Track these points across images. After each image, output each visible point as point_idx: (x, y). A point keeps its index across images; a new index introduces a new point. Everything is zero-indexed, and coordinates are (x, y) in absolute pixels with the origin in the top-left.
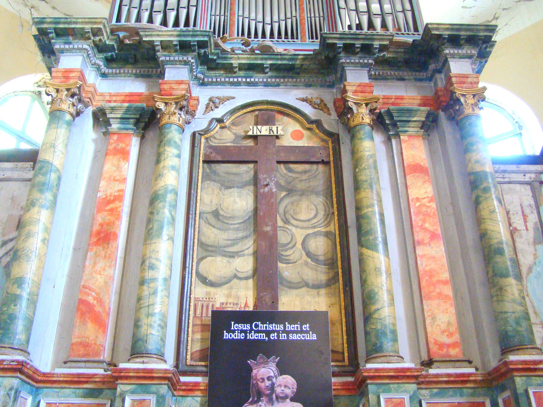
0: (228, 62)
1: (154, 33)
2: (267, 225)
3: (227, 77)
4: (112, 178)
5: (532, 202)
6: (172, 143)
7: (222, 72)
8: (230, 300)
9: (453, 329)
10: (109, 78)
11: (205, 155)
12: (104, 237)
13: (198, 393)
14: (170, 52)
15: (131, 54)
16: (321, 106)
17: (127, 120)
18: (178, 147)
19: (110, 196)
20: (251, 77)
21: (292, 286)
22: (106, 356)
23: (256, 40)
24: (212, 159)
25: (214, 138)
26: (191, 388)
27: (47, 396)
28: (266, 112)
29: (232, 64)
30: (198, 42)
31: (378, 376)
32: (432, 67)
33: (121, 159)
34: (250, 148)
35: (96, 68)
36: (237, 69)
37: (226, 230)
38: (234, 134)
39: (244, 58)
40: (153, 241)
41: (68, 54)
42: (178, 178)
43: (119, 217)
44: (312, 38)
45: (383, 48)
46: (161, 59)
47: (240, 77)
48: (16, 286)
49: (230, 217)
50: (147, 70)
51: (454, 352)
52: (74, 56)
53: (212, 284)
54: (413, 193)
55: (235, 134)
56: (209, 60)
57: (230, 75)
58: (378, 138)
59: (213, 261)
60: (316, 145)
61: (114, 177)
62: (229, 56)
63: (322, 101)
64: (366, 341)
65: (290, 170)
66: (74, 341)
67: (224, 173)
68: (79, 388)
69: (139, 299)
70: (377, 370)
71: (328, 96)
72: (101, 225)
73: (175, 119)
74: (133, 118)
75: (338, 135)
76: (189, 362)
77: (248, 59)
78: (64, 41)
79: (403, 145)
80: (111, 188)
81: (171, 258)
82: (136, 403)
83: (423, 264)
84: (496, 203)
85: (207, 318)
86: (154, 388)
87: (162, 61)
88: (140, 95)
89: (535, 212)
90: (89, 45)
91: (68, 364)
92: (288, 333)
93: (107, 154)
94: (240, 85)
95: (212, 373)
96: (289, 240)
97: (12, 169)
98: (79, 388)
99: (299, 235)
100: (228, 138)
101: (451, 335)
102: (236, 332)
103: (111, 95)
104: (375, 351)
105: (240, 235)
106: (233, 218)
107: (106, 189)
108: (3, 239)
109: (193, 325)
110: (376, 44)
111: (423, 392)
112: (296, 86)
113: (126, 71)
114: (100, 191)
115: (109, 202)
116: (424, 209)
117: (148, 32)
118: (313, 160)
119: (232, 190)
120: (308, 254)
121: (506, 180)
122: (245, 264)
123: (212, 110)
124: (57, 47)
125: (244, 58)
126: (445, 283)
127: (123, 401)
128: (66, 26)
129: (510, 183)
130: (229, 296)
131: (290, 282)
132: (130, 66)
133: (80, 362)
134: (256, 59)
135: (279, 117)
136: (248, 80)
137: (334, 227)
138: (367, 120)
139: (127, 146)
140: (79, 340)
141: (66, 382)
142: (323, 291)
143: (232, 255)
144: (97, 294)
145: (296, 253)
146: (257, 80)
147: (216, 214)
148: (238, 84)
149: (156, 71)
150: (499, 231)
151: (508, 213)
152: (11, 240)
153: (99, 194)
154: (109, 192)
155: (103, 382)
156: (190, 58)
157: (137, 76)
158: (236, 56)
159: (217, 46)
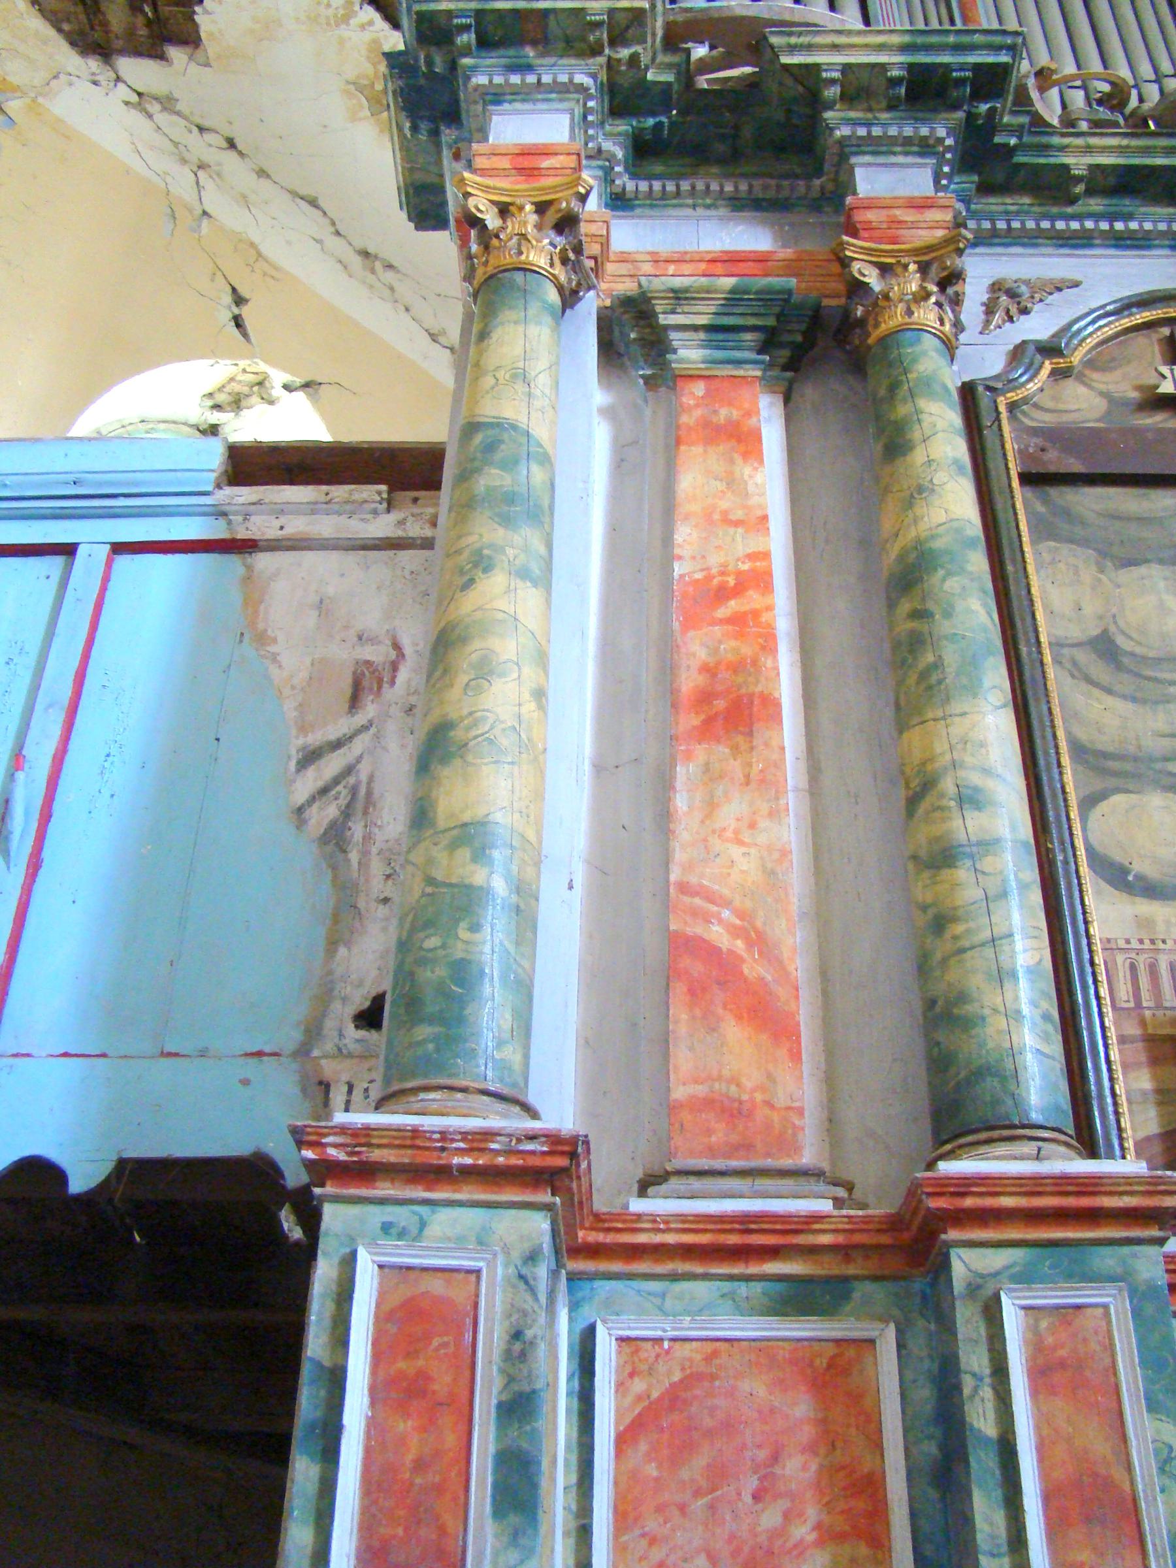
0: (1052, 161)
1: (819, 40)
3: (1045, 216)
4: (716, 517)
6: (937, 388)
7: (1027, 200)
10: (638, 211)
11: (1022, 454)
14: (870, 110)
17: (730, 336)
19: (722, 573)
20: (1129, 217)
24: (1052, 469)
27: (611, 1307)
29: (1066, 168)
30: (977, 67)
33: (738, 459)
35: (601, 167)
36: (1079, 189)
37: (1156, 703)
38: (1101, 394)
39: (1104, 150)
40: (956, 707)
41: (518, 105)
43: (768, 643)
46: (838, 133)
47: (1090, 216)
48: (464, 853)
49: (1159, 660)
50: (773, 182)
52: (541, 112)
57: (1055, 210)
59: (1134, 807)
61: (725, 513)
62: (1056, 140)
66: (679, 1093)
67: (1099, 514)
68: (748, 1278)
74: (754, 329)
77: (1121, 150)
78: (503, 61)
80: (719, 547)
82: (1044, 1324)
85: (1160, 1013)
86: (1106, 1260)
87: (842, 142)
90: (594, 76)
91: (674, 1183)
94: (1090, 246)
97: (313, 509)
98: (748, 1278)
100: (1084, 406)
103: (656, 259)
108: (301, 742)
109: (1122, 1040)
113: (700, 186)
114: (680, 558)
115: (722, 594)
117: (800, 34)
119: (1143, 570)
123: (1011, 319)
125: (1104, 150)
127: (992, 1313)
132: (714, 170)
133: (722, 1173)
134: (1147, 151)
136: (1119, 226)
139: (748, 414)
140: (700, 1090)
141: (687, 1252)
144: (741, 915)
146: (1148, 226)
147: (1105, 646)
149: (809, 188)
152: (337, 745)
153: (678, 569)
154: (715, 560)
155: (844, 1251)
156: (942, 129)
157: (740, 204)
158: (1079, 141)
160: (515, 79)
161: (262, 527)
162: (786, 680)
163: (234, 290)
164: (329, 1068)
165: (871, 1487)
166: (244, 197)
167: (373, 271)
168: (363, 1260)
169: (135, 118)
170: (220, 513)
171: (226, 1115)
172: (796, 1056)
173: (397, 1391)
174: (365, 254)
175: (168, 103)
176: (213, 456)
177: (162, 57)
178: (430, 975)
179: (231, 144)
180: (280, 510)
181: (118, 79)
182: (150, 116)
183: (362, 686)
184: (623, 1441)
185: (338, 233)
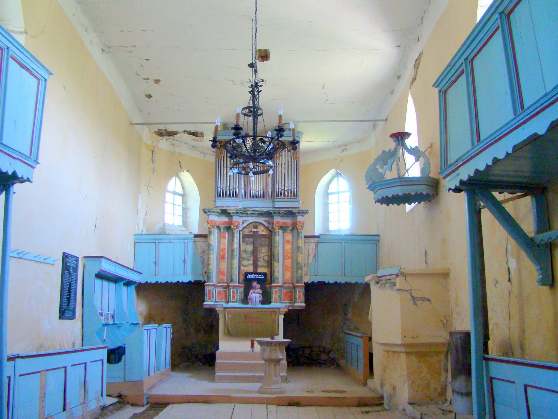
12: (223, 258)
15: (224, 212)
16: (269, 223)
21: (260, 267)
26: (241, 287)
28: (256, 225)
58: (281, 232)
69: (232, 271)
71: (270, 219)
83: (286, 264)
95: (245, 284)
99: (262, 255)
102: (249, 276)
107: (222, 247)
122: (251, 262)
137: (269, 254)
143: (249, 260)
145: (261, 260)
147: (245, 251)
150: (300, 260)
168: (207, 289)
171: (200, 278)
176: (193, 236)
183: (204, 252)
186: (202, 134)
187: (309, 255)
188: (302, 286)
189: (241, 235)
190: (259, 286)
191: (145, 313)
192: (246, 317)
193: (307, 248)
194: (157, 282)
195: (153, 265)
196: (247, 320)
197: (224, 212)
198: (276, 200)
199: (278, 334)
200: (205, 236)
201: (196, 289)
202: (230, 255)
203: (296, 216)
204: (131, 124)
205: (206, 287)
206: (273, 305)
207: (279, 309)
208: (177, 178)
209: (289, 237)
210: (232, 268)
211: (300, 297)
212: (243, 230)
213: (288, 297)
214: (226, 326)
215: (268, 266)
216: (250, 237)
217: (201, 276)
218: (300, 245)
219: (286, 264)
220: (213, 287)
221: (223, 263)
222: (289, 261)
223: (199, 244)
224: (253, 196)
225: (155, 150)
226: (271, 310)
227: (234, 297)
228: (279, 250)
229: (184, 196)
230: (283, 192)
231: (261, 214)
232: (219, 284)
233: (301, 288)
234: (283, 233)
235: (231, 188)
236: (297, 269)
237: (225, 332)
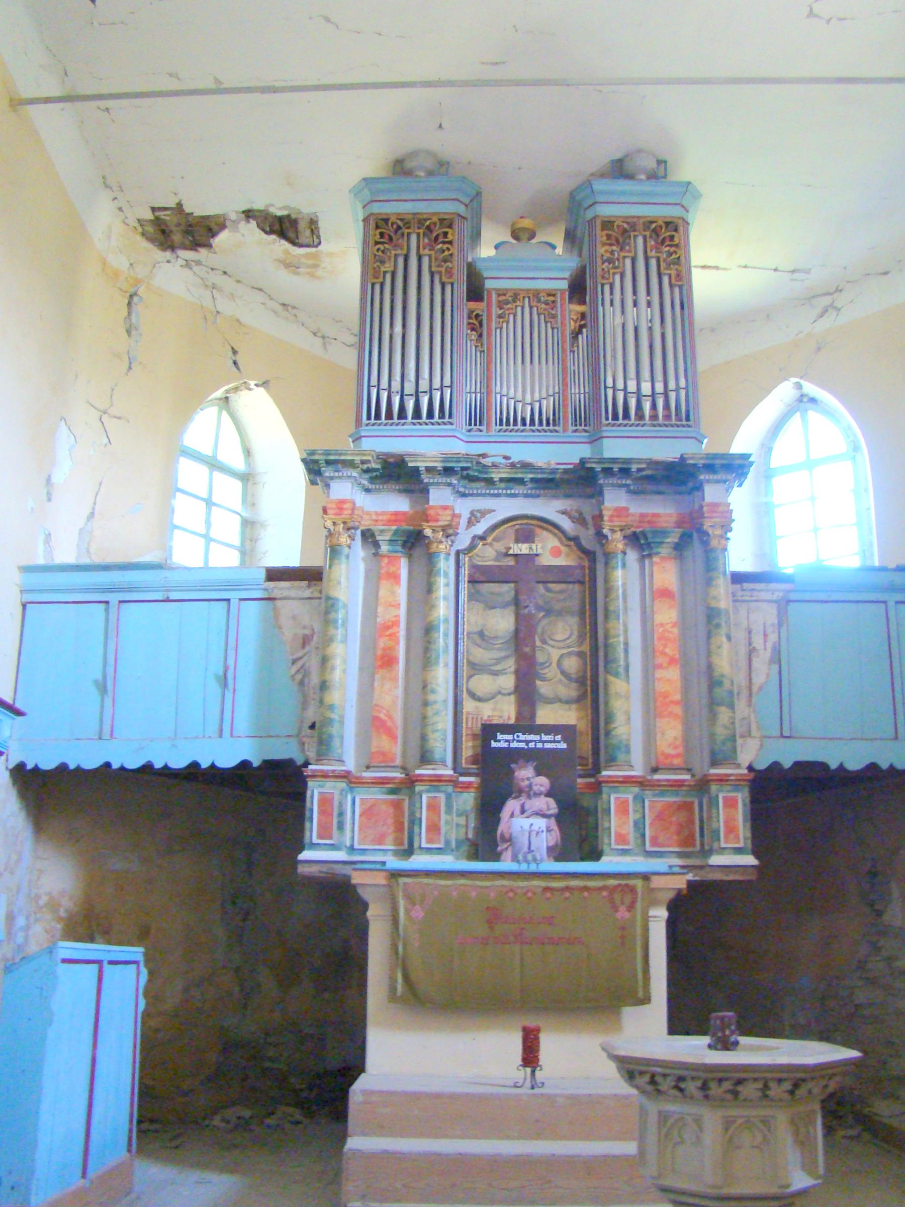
2: (527, 646)
5: (776, 622)
7: (483, 484)
8: (496, 714)
9: (678, 743)
12: (388, 661)
13: (472, 790)
15: (395, 472)
16: (580, 520)
18: (446, 575)
20: (511, 489)
21: (549, 701)
22: (398, 762)
23: (516, 428)
25: (477, 555)
28: (526, 528)
31: (611, 781)
32: (690, 485)
34: (512, 566)
42: (447, 608)
43: (398, 643)
44: (576, 425)
45: (639, 470)
51: (677, 762)
53: (480, 700)
54: (659, 618)
55: (496, 551)
56: (469, 474)
58: (632, 556)
60: (573, 563)
63: (581, 514)
64: (606, 752)
65: (548, 590)
66: (374, 750)
69: (424, 717)
70: (610, 776)
71: (587, 508)
72: (384, 649)
73: (442, 546)
75: (594, 553)
76: (464, 766)
79: (655, 568)
81: (447, 682)
84: (724, 639)
86: (443, 788)
88: (405, 513)
89: (777, 631)
91: (372, 769)
92: (544, 742)
93: (380, 578)
96: (546, 659)
97: (289, 589)
99: (555, 654)
101: (676, 747)
102: (501, 742)
103: (377, 513)
104: (612, 761)
105: (503, 654)
106: (496, 638)
107: (384, 615)
110: (634, 467)
111: (647, 792)
112: (555, 497)
115: (388, 628)
116: (667, 634)
118: (570, 580)
120: (563, 672)
121: (754, 598)
122: (508, 682)
124: (327, 474)
126: (676, 703)
128: (337, 457)
129: (756, 601)
130: (494, 710)
131: (546, 698)
134: (516, 473)
135: (538, 530)
136: (509, 492)
137: (586, 648)
138: (620, 546)
141: (373, 783)
142: (574, 706)
143: (496, 674)
144: (387, 711)
145: (552, 672)
147: (481, 634)
148: (498, 495)
150: (723, 664)
151: (750, 632)
152: (301, 658)
153: (378, 620)
154: (387, 617)
155: (401, 783)
157: (400, 491)
159: (478, 463)
160: (336, 474)
161: (276, 594)
162: (401, 652)
163: (233, 348)
164: (305, 739)
165: (402, 823)
166: (232, 295)
167: (287, 310)
168: (315, 791)
169: (187, 271)
170: (265, 590)
171: (284, 750)
172: (397, 743)
173: (322, 812)
174: (284, 305)
175: (198, 263)
176: (263, 575)
177: (196, 250)
178: (324, 737)
179: (225, 273)
180: (281, 589)
181: (178, 257)
182: (191, 269)
183: (305, 641)
184: (360, 816)
185: (272, 299)
186: (313, 224)
187: (751, 652)
188: (740, 779)
189: (465, 572)
190: (542, 783)
191: (67, 904)
192: (494, 916)
193: (745, 624)
194: (108, 765)
195: (95, 696)
196: (500, 929)
197: (395, 472)
198: (607, 431)
199: (646, 1000)
200: (310, 576)
201: (271, 792)
202: (418, 649)
203: (699, 488)
204: (17, 103)
205: (311, 784)
206: (609, 863)
207: (646, 877)
208: (224, 413)
209: (666, 574)
210: (426, 704)
211: (731, 830)
212: (472, 547)
213: (673, 828)
214: (400, 961)
215: (579, 700)
216: (501, 576)
217: (293, 742)
218: (722, 605)
219: (660, 687)
220: (343, 785)
221: (388, 686)
222: (673, 674)
223: (287, 609)
224: (511, 422)
225: (142, 291)
226: (612, 882)
227: (434, 828)
228: (627, 629)
229: (247, 478)
230: (633, 402)
231: (548, 483)
232: (367, 774)
233: (736, 788)
234: (642, 559)
235: (424, 385)
236: (713, 703)
237: (393, 988)
